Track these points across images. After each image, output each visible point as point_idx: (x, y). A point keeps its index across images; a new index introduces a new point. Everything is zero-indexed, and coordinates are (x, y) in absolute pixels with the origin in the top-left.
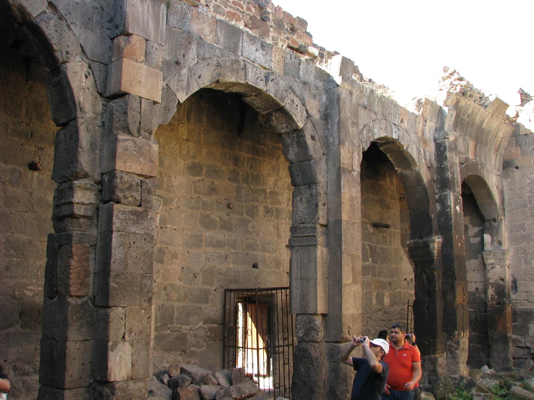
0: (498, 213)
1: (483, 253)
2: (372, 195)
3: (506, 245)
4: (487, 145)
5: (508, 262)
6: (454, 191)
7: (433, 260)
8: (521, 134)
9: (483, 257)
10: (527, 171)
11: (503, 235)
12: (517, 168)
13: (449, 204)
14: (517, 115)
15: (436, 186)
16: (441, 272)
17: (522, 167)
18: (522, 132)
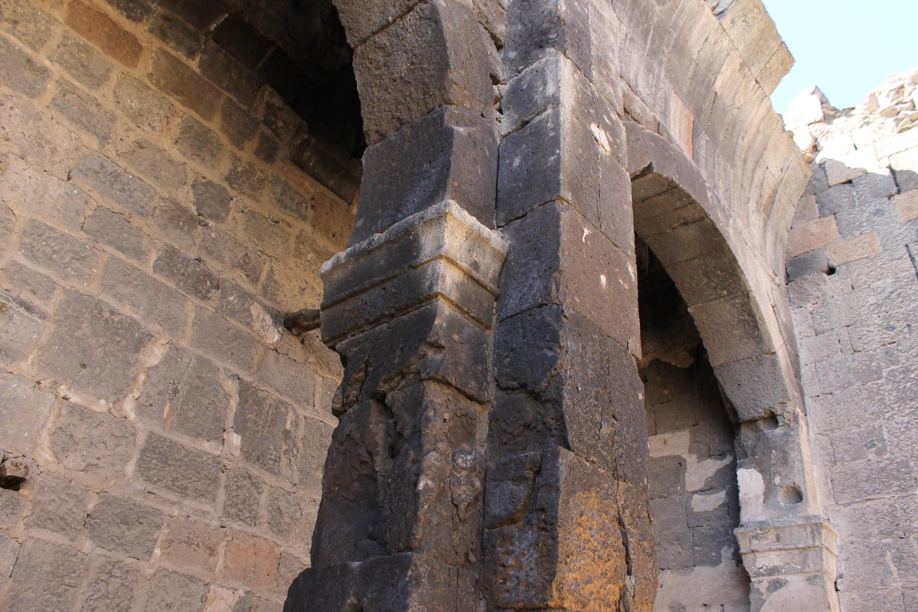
0: (785, 391)
1: (737, 531)
2: (308, 228)
3: (817, 503)
4: (733, 166)
5: (832, 566)
6: (583, 66)
7: (428, 319)
8: (831, 183)
9: (737, 548)
10: (866, 270)
11: (807, 466)
12: (831, 271)
13: (551, 90)
14: (816, 148)
15: (504, 60)
16: (483, 415)
17: (847, 264)
18: (835, 178)
